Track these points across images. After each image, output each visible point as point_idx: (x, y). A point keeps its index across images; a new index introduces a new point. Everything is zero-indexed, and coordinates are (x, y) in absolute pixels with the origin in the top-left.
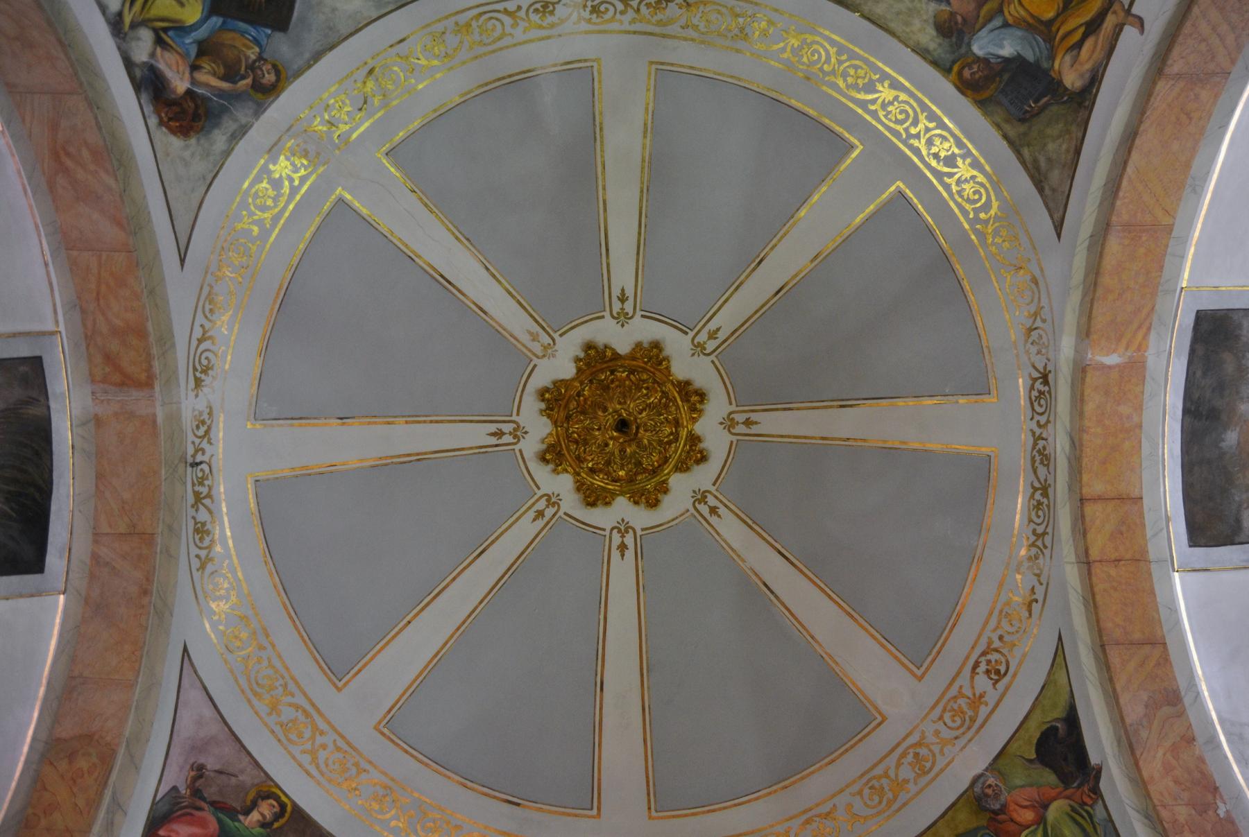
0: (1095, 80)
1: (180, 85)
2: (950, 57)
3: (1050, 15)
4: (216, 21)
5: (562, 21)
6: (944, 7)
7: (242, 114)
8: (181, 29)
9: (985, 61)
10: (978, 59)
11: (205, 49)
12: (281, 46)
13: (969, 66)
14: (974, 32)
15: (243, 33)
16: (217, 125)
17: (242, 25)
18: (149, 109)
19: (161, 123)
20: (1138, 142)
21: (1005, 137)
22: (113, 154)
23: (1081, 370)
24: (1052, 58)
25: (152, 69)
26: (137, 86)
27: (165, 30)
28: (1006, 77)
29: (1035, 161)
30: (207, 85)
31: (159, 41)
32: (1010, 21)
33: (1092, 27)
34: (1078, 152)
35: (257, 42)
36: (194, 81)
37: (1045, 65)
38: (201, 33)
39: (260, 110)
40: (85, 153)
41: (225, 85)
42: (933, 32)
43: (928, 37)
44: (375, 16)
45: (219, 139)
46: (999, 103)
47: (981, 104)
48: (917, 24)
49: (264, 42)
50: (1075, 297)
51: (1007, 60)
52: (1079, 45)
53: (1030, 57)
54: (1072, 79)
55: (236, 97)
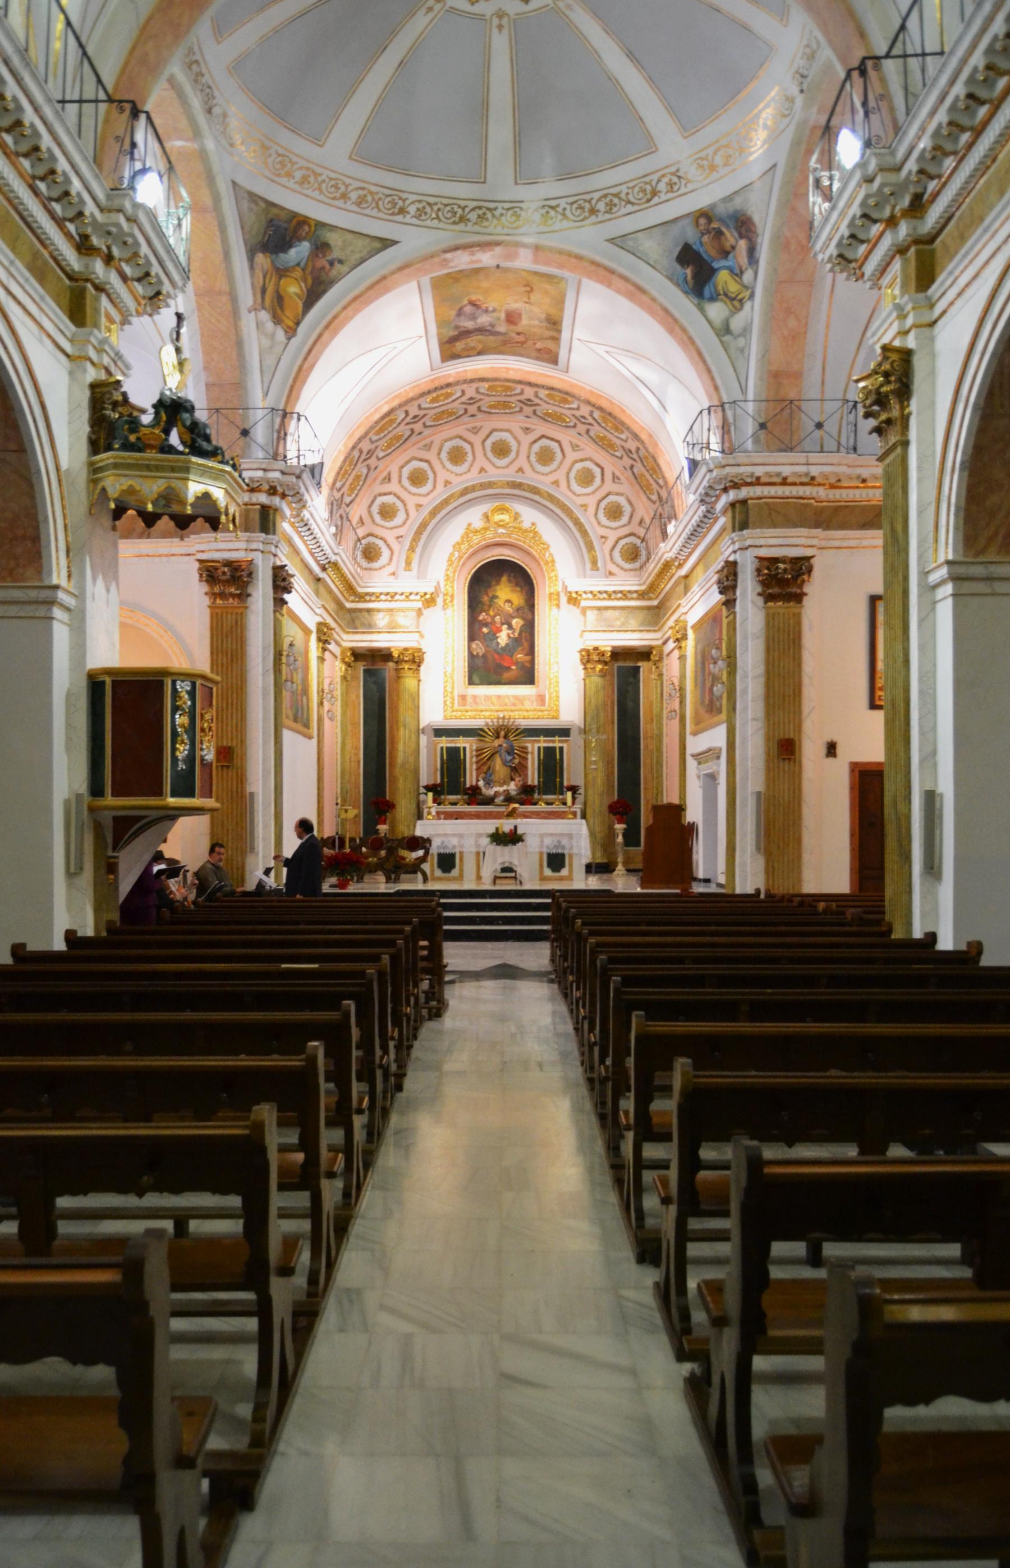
0: (252, 267)
1: (743, 244)
2: (318, 233)
3: (283, 281)
4: (715, 265)
5: (536, 210)
6: (329, 258)
7: (722, 210)
8: (731, 270)
9: (300, 240)
10: (304, 239)
11: (725, 254)
12: (691, 235)
13: (307, 233)
14: (311, 252)
15: (706, 252)
16: (736, 211)
17: (705, 256)
18: (758, 247)
19: (757, 236)
20: (222, 256)
21: (274, 205)
22: (781, 244)
23: (197, 134)
24: (272, 262)
25: (750, 263)
26: (757, 262)
27: (737, 275)
28: (288, 239)
29: (257, 204)
30: (732, 235)
31: (742, 272)
32: (297, 268)
33: (264, 290)
34: (242, 228)
35: (701, 243)
36: (737, 241)
37: (274, 256)
38: (723, 263)
39: (713, 206)
40: (793, 247)
41: (724, 229)
42: (331, 242)
43: (333, 238)
44: (639, 234)
45: (737, 203)
46: (285, 222)
47: (295, 215)
48: (340, 243)
49: (698, 243)
50: (216, 168)
51: (291, 247)
52: (265, 277)
53: (281, 255)
54: (260, 258)
55: (720, 220)
